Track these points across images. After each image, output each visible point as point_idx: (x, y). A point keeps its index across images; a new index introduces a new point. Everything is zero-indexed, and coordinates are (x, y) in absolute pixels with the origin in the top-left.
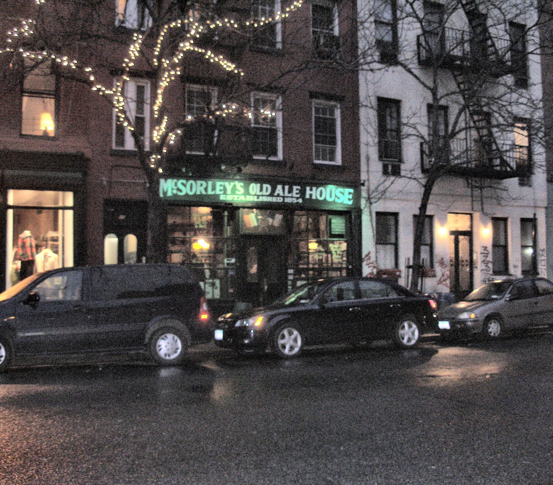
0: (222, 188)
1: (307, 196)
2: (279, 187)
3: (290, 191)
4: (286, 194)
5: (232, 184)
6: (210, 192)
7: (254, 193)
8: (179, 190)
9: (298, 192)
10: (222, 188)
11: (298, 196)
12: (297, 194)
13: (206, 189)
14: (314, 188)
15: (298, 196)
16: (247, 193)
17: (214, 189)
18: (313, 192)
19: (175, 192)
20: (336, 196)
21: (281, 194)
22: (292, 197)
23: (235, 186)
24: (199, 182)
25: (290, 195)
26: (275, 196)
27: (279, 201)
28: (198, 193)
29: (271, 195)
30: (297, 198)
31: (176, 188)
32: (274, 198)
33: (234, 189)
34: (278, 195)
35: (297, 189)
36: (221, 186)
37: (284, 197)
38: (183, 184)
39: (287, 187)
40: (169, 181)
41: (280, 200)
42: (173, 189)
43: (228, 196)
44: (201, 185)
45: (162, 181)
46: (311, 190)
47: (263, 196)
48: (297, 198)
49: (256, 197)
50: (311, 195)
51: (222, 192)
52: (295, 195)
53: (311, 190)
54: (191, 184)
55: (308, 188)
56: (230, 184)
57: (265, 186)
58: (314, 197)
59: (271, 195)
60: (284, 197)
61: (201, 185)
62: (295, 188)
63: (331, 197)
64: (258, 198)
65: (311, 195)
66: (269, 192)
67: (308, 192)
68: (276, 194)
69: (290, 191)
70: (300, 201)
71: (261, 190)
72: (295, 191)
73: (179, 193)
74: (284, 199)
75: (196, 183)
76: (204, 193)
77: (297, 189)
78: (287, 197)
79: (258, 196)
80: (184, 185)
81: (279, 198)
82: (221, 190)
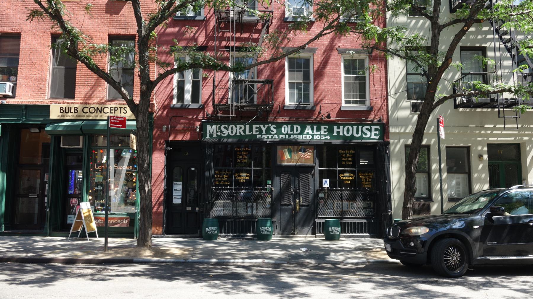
0: (258, 130)
2: (309, 127)
3: (319, 129)
5: (267, 126)
6: (248, 133)
7: (286, 133)
8: (221, 131)
9: (326, 130)
10: (258, 130)
12: (325, 132)
13: (244, 131)
14: (341, 127)
15: (326, 133)
16: (279, 133)
17: (251, 130)
18: (341, 130)
19: (219, 134)
20: (362, 132)
22: (320, 135)
24: (238, 126)
25: (319, 133)
27: (308, 138)
28: (238, 134)
30: (325, 136)
31: (220, 130)
32: (304, 136)
33: (268, 131)
34: (308, 134)
35: (325, 128)
36: (257, 128)
37: (313, 135)
38: (225, 128)
39: (315, 127)
40: (214, 126)
41: (309, 137)
42: (217, 132)
43: (263, 136)
44: (240, 128)
45: (209, 127)
46: (338, 128)
47: (293, 134)
48: (325, 136)
49: (287, 136)
50: (338, 133)
51: (258, 133)
53: (338, 128)
54: (232, 128)
55: (335, 127)
57: (295, 127)
58: (341, 134)
62: (323, 127)
63: (358, 133)
68: (305, 133)
71: (292, 130)
74: (313, 137)
75: (236, 127)
76: (243, 134)
77: (325, 128)
78: (316, 135)
80: (227, 129)
81: (308, 136)
82: (256, 131)
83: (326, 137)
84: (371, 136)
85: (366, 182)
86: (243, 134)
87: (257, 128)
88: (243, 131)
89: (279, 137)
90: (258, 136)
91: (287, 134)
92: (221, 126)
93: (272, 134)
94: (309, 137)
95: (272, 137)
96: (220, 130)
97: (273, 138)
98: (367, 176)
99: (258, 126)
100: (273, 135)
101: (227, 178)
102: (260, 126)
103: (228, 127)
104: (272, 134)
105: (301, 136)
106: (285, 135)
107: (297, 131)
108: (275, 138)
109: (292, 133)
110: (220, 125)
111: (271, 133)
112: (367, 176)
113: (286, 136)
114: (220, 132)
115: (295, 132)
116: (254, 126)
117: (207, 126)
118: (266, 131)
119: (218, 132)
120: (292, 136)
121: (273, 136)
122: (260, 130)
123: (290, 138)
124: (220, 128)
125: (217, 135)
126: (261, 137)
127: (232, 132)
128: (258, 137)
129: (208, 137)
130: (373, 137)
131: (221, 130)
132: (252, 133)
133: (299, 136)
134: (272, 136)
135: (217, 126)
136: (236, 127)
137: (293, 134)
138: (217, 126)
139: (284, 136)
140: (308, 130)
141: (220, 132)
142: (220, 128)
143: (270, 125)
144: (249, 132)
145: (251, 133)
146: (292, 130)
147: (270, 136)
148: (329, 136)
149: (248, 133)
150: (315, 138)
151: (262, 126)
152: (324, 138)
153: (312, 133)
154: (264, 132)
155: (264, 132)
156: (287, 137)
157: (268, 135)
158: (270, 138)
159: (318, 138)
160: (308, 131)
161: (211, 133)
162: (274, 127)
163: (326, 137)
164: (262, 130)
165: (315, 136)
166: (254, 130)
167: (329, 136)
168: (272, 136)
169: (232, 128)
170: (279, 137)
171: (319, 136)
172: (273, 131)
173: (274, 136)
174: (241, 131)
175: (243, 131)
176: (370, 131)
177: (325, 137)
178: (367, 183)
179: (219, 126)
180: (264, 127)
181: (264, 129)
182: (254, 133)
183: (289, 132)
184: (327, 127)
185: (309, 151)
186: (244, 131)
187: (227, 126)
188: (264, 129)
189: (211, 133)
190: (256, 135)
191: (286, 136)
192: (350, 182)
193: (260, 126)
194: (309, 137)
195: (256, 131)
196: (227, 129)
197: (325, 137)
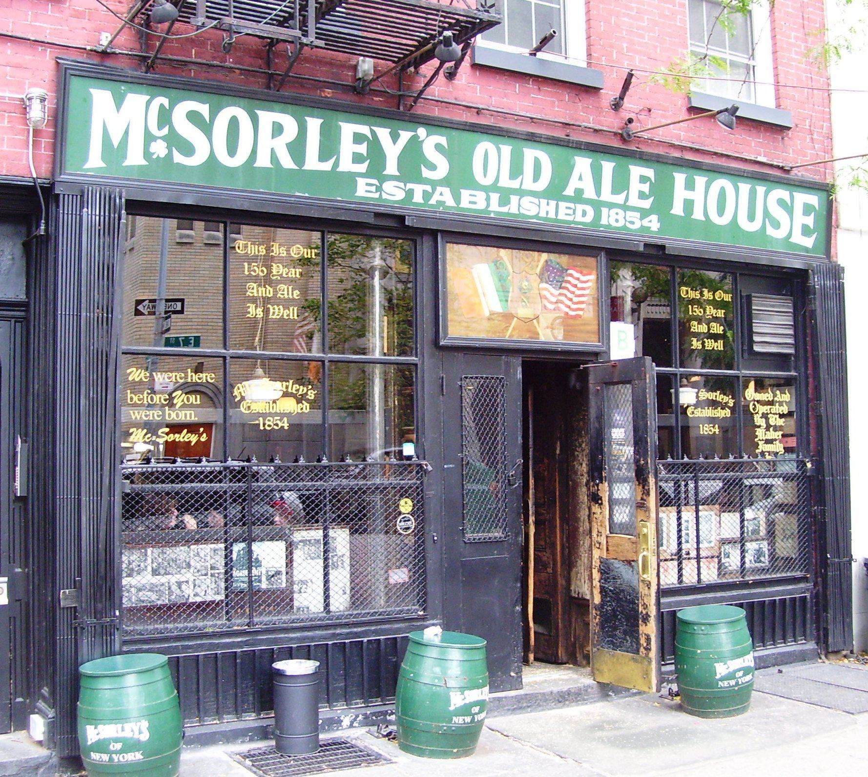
0: (362, 149)
1: (678, 209)
3: (621, 184)
4: (607, 195)
5: (405, 136)
6: (312, 162)
7: (488, 181)
8: (175, 141)
9: (646, 188)
10: (362, 149)
11: (647, 204)
12: (642, 196)
13: (297, 148)
15: (647, 204)
18: (697, 196)
19: (159, 149)
20: (766, 214)
21: (590, 193)
22: (625, 207)
23: (415, 144)
24: (267, 117)
25: (620, 199)
26: (567, 199)
27: (579, 218)
28: (263, 161)
29: (555, 192)
30: (644, 213)
31: (165, 131)
32: (563, 205)
34: (578, 197)
35: (643, 179)
36: (358, 138)
38: (193, 117)
40: (136, 100)
42: (149, 138)
43: (388, 186)
44: (278, 130)
46: (690, 185)
47: (521, 193)
49: (495, 197)
50: (689, 205)
51: (362, 168)
52: (634, 201)
53: (690, 185)
54: (234, 123)
56: (395, 137)
58: (698, 214)
59: (555, 192)
60: (597, 205)
61: (278, 130)
63: (751, 217)
64: (504, 201)
65: (689, 205)
66: (543, 183)
67: (680, 193)
68: (569, 191)
69: (621, 184)
70: (653, 223)
71: (516, 170)
72: (635, 186)
73: (178, 158)
74: (598, 215)
75: (255, 121)
76: (287, 162)
77: (643, 179)
78: (611, 206)
79: (505, 196)
80: (207, 128)
81: (580, 207)
82: (357, 158)
83: (645, 222)
84: (790, 234)
85: (768, 428)
86: (287, 162)
87: (358, 138)
88: (290, 146)
89: (457, 198)
90: (361, 182)
91: (494, 187)
92: (173, 105)
93: (426, 181)
94: (584, 213)
95: (427, 196)
96: (165, 131)
97: (433, 201)
98: (771, 403)
99: (364, 130)
100: (434, 184)
101: (192, 406)
102: (372, 131)
103: (213, 114)
104: (426, 181)
105: (553, 203)
106: (486, 189)
107: (536, 177)
108: (441, 203)
109: (515, 184)
110: (165, 101)
111: (426, 173)
112: (771, 403)
113: (488, 199)
114: (163, 138)
115: (528, 184)
116: (348, 129)
117: (88, 100)
118: (401, 159)
119: (155, 139)
120: (514, 199)
121: (434, 190)
122: (376, 155)
123: (504, 209)
124: (165, 117)
125: (147, 154)
126: (379, 189)
127: (232, 150)
128: (364, 190)
129: (95, 161)
130: (798, 238)
131: (172, 129)
132: (336, 164)
133: (544, 202)
134: (429, 188)
135: (148, 103)
136: (255, 121)
137: (521, 193)
138: (148, 103)
139: (481, 196)
140: (580, 178)
141: (163, 138)
142: (165, 117)
143: (422, 131)
144: (323, 158)
145: (327, 166)
146: (516, 170)
147: (418, 190)
148: (654, 218)
149: (312, 162)
150: (604, 221)
151: (383, 134)
152: (637, 225)
153: (595, 197)
154: (391, 168)
155: (391, 168)
156: (495, 206)
157: (410, 186)
158: (418, 198)
159: (617, 221)
160: (580, 185)
161: (116, 142)
162: (438, 147)
163: (645, 222)
164: (383, 157)
165: (605, 211)
166: (347, 147)
167: (654, 218)
168: (429, 188)
169: (234, 123)
170: (457, 198)
171: (621, 212)
172: (433, 167)
173: (439, 189)
174: (281, 145)
175: (290, 146)
176: (789, 209)
177: (641, 219)
178: (772, 435)
179: (162, 106)
180: (395, 137)
181: (392, 151)
182: (346, 165)
183: (505, 182)
184: (649, 173)
185: (578, 279)
186: (297, 148)
187: (204, 109)
188: (392, 151)
189: (116, 142)
190: (352, 177)
191: (488, 199)
192: (717, 431)
193: (373, 133)
194: (584, 213)
195: (357, 158)
196: (207, 128)
197: (641, 219)
